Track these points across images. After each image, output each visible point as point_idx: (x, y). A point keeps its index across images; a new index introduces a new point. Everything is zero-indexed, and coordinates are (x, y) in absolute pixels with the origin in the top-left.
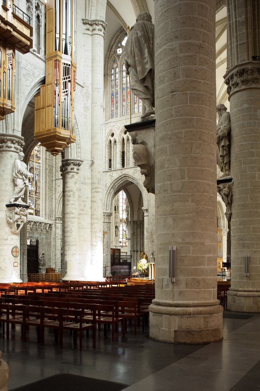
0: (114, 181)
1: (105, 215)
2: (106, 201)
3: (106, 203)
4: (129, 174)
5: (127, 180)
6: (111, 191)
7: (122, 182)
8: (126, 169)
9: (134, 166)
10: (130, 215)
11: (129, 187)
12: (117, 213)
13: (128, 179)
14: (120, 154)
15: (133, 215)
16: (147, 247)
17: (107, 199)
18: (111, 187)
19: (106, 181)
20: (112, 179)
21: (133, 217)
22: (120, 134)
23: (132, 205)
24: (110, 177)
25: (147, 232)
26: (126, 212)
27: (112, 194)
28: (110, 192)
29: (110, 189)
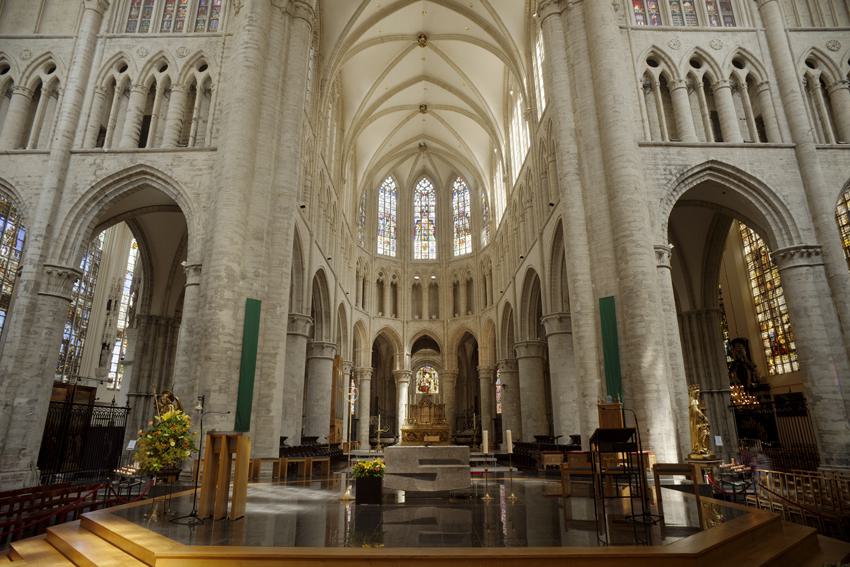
0: (104, 180)
1: (55, 273)
2: (66, 233)
3: (64, 238)
4: (156, 167)
5: (148, 185)
6: (89, 209)
7: (131, 187)
8: (148, 152)
9: (175, 148)
10: (143, 299)
11: (149, 220)
12: (111, 315)
13: (150, 183)
14: (138, 115)
15: (151, 300)
16: (185, 379)
17: (72, 227)
18: (90, 196)
19: (76, 178)
20: (98, 173)
21: (150, 306)
22: (148, 67)
23: (152, 275)
24: (94, 168)
25: (190, 332)
26: (131, 293)
27: (91, 218)
28: (83, 210)
29: (86, 200)
